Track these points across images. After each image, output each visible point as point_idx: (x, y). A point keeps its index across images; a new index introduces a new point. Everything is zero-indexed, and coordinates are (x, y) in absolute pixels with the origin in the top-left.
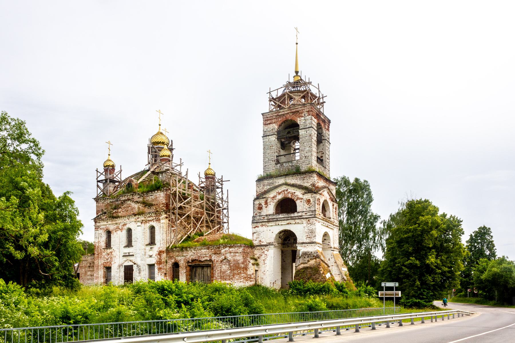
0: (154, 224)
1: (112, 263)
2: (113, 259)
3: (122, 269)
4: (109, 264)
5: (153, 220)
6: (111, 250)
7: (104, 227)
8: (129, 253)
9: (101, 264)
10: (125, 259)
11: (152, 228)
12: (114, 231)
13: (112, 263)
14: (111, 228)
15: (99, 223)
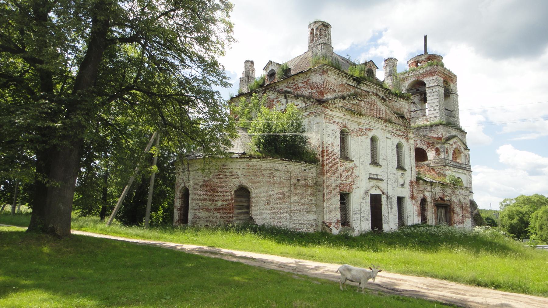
0: (403, 141)
1: (354, 187)
2: (355, 180)
3: (368, 200)
4: (348, 187)
5: (401, 136)
6: (351, 165)
7: (340, 121)
8: (377, 175)
9: (337, 186)
10: (372, 183)
11: (399, 147)
12: (355, 134)
13: (354, 187)
14: (352, 126)
15: (331, 110)
